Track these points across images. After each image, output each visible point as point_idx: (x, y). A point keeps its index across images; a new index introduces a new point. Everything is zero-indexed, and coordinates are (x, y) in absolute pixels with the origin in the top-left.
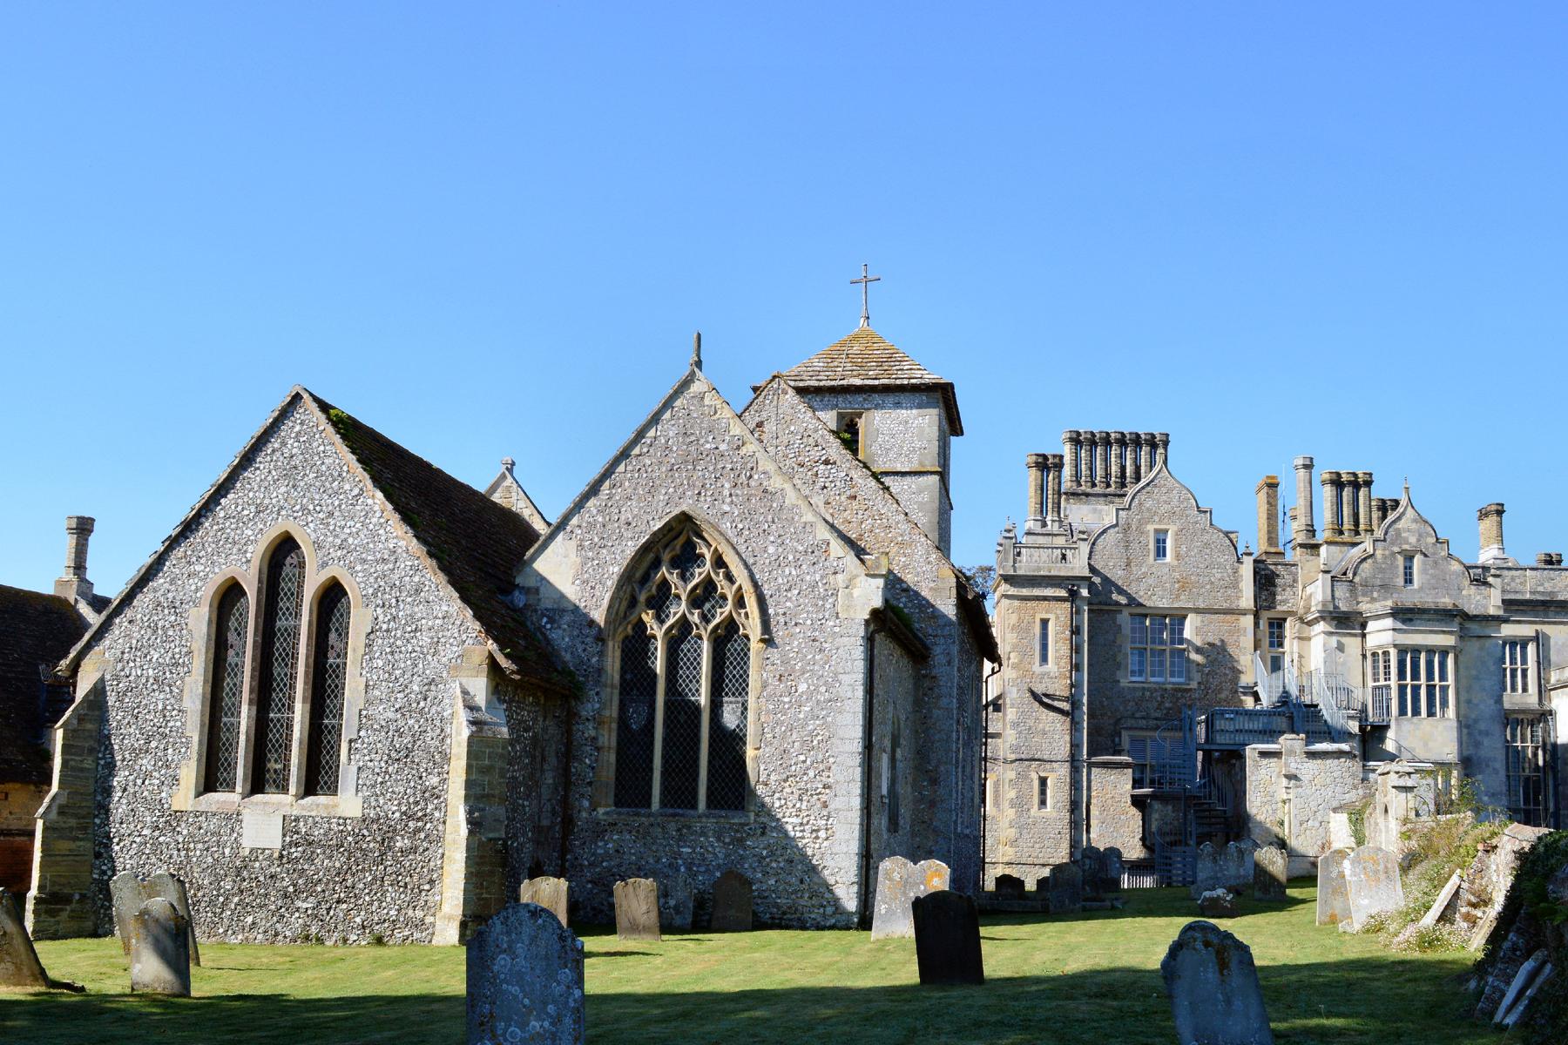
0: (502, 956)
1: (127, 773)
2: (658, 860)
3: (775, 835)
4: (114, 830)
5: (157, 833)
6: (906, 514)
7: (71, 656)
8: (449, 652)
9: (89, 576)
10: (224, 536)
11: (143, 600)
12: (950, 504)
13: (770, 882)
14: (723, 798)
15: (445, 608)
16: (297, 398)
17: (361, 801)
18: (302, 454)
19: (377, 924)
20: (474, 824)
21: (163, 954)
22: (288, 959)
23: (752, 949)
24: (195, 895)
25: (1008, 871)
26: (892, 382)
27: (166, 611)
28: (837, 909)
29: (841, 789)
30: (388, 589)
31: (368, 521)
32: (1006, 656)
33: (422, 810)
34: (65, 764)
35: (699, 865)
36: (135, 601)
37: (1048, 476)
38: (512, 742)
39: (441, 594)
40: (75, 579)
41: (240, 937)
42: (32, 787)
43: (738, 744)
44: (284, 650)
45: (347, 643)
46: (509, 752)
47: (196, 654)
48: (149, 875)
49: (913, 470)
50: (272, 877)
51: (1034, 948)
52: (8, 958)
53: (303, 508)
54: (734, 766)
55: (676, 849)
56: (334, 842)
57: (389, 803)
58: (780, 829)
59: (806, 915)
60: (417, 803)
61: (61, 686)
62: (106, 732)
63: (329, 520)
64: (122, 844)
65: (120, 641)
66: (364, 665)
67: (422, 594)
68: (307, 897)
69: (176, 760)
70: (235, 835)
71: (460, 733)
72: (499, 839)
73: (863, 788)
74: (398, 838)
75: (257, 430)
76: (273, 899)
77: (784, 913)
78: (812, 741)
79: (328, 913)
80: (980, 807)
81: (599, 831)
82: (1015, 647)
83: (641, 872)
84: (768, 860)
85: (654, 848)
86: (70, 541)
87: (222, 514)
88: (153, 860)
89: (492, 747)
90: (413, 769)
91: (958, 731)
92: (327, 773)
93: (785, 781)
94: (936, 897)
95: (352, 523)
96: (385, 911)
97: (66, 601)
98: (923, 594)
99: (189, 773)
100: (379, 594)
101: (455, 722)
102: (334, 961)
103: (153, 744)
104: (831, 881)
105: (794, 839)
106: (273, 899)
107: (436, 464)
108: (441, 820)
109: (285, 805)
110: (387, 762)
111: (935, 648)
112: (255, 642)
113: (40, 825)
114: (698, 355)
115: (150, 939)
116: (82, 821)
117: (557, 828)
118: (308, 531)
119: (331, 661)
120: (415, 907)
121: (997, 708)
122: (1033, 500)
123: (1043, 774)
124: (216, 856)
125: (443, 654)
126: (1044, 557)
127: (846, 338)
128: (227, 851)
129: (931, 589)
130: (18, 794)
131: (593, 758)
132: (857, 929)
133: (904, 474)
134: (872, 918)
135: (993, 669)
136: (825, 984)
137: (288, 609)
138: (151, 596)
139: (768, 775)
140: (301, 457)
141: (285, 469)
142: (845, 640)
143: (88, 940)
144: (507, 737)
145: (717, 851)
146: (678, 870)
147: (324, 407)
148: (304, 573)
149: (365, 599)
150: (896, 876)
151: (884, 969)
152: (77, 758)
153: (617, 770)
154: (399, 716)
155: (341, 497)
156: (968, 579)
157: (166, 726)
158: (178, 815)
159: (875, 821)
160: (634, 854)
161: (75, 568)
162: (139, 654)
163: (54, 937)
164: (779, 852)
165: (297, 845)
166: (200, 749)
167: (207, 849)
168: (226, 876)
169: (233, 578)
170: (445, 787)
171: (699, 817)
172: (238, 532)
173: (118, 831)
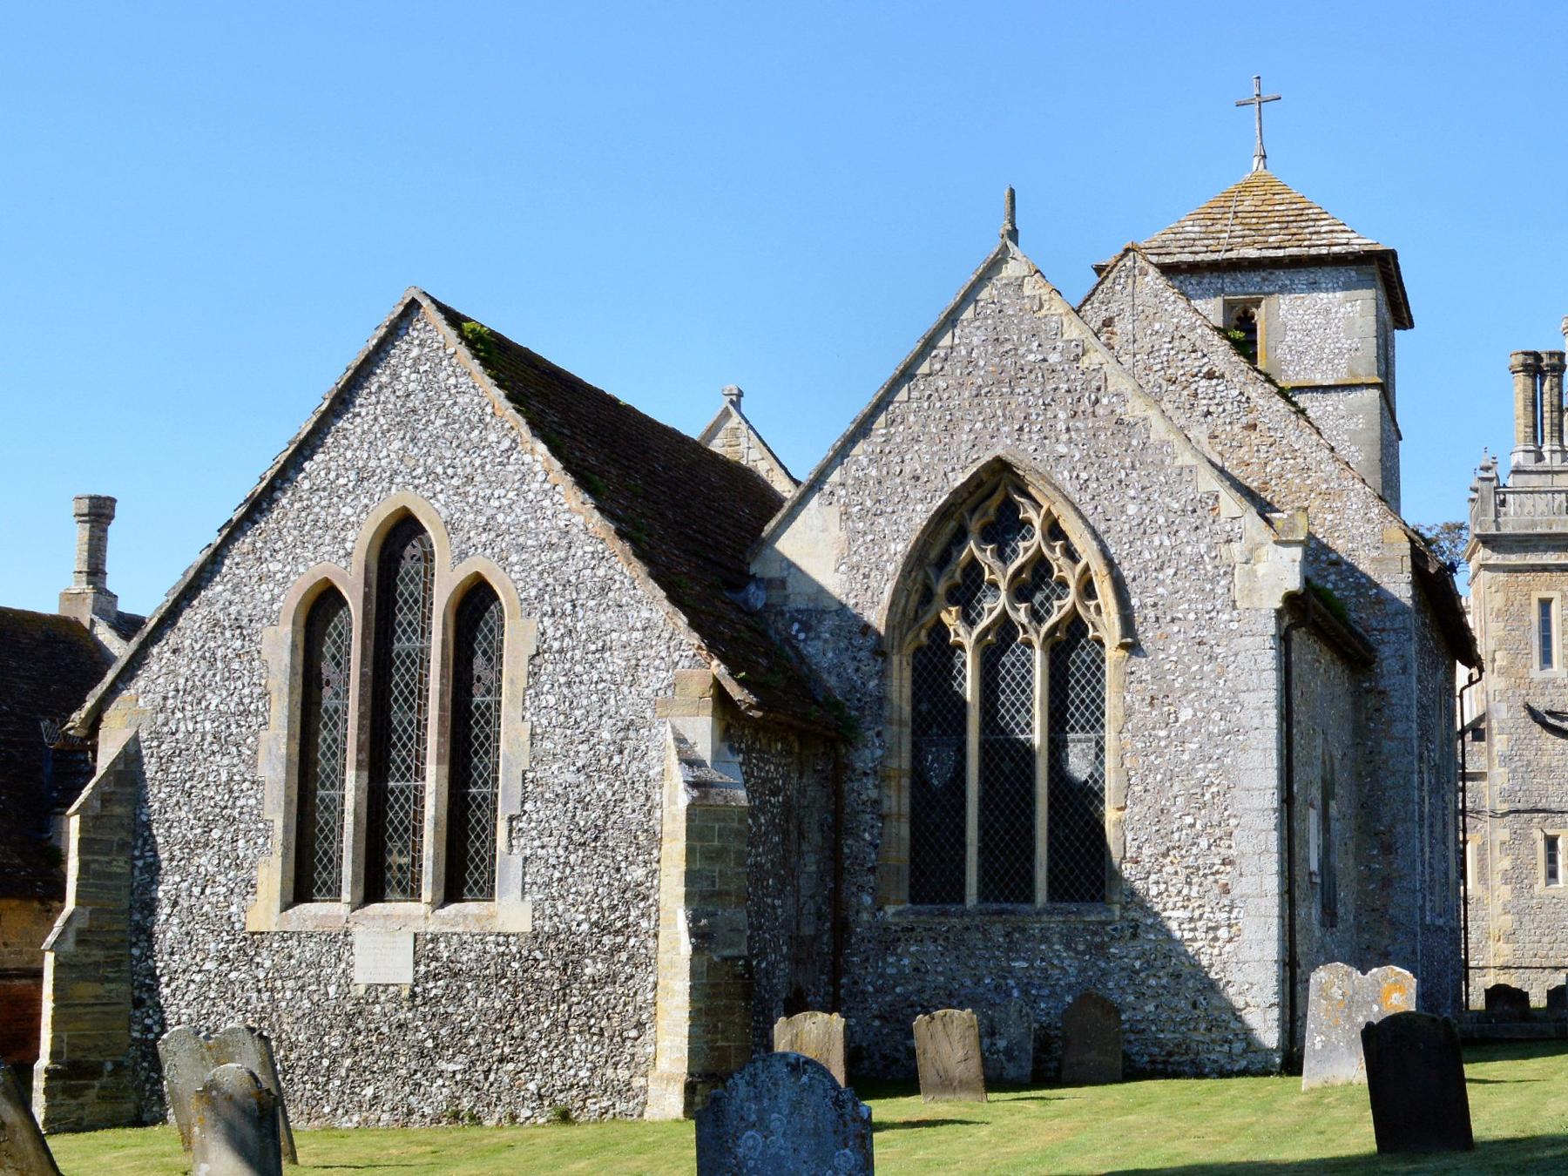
0: (749, 1133)
1: (178, 879)
2: (978, 981)
3: (1152, 937)
4: (161, 965)
5: (225, 967)
6: (1332, 449)
7: (88, 705)
8: (652, 681)
9: (111, 585)
10: (311, 517)
11: (193, 619)
12: (1398, 431)
13: (1147, 1009)
14: (1072, 884)
15: (645, 614)
16: (412, 307)
17: (530, 907)
18: (423, 390)
19: (561, 1091)
20: (701, 937)
21: (241, 1148)
22: (429, 1149)
23: (1125, 1110)
24: (286, 1058)
25: (1503, 979)
26: (1304, 251)
27: (228, 634)
28: (1249, 1044)
29: (1249, 865)
30: (559, 589)
31: (525, 487)
32: (1490, 657)
33: (621, 918)
34: (84, 867)
35: (1040, 987)
36: (181, 620)
37: (1542, 385)
38: (752, 812)
39: (639, 593)
40: (89, 590)
41: (356, 1118)
42: (36, 905)
43: (1092, 803)
44: (407, 685)
45: (500, 672)
46: (750, 828)
47: (274, 695)
48: (215, 1031)
49: (1340, 382)
50: (400, 1026)
51: (1546, 1093)
52: (9, 1162)
53: (428, 472)
54: (1087, 837)
55: (1004, 964)
56: (492, 971)
57: (573, 910)
58: (1160, 928)
59: (1203, 1056)
60: (614, 908)
61: (74, 752)
62: (144, 818)
63: (468, 488)
64: (173, 986)
65: (161, 680)
66: (528, 703)
67: (611, 595)
68: (454, 1055)
69: (251, 856)
70: (343, 965)
71: (675, 801)
72: (739, 958)
73: (1281, 862)
74: (588, 961)
75: (354, 357)
76: (403, 1059)
77: (1170, 1054)
78: (1203, 795)
79: (486, 1078)
80: (1459, 885)
81: (888, 941)
82: (1502, 643)
83: (954, 999)
84: (1143, 975)
85: (972, 963)
86: (81, 533)
87: (306, 485)
88: (222, 1007)
89: (724, 820)
90: (606, 857)
91: (1421, 772)
92: (477, 868)
93: (1165, 855)
94: (1396, 1022)
95: (503, 492)
96: (572, 1072)
97: (77, 624)
98: (1361, 567)
99: (271, 875)
100: (547, 597)
101: (666, 784)
102: (497, 1150)
103: (216, 834)
104: (1239, 1002)
105: (1180, 942)
106: (403, 1059)
107: (625, 399)
108: (651, 932)
109: (418, 917)
110: (567, 848)
111: (1381, 647)
112: (362, 675)
113: (49, 961)
114: (1012, 222)
115: (220, 1126)
116: (112, 952)
117: (825, 938)
118: (437, 505)
119: (477, 699)
120: (616, 1065)
121: (1479, 735)
122: (1522, 421)
123: (1550, 832)
124: (316, 998)
125: (644, 683)
126: (1541, 507)
127: (1232, 188)
128: (332, 990)
129: (1373, 560)
130: (16, 915)
131: (876, 831)
132: (1280, 1074)
133: (1326, 389)
134: (1301, 1057)
135: (1470, 677)
136: (1235, 1159)
137: (410, 624)
138: (204, 611)
139: (1139, 848)
140: (422, 395)
141: (399, 414)
142: (1247, 641)
143: (129, 1131)
144: (746, 804)
145: (1066, 964)
146: (1009, 995)
147: (454, 319)
148: (433, 568)
149: (525, 605)
150: (1337, 993)
151: (1322, 1133)
152: (101, 858)
153: (912, 847)
154: (582, 778)
155: (484, 453)
156: (1428, 543)
157: (234, 806)
158: (257, 938)
159: (1301, 911)
160: (942, 973)
161: (89, 574)
162: (190, 699)
163: (77, 1127)
164: (1158, 963)
165: (436, 977)
166: (285, 839)
167: (302, 989)
168: (331, 1027)
169: (327, 580)
170: (655, 882)
171: (1038, 914)
172: (331, 510)
173: (167, 966)
